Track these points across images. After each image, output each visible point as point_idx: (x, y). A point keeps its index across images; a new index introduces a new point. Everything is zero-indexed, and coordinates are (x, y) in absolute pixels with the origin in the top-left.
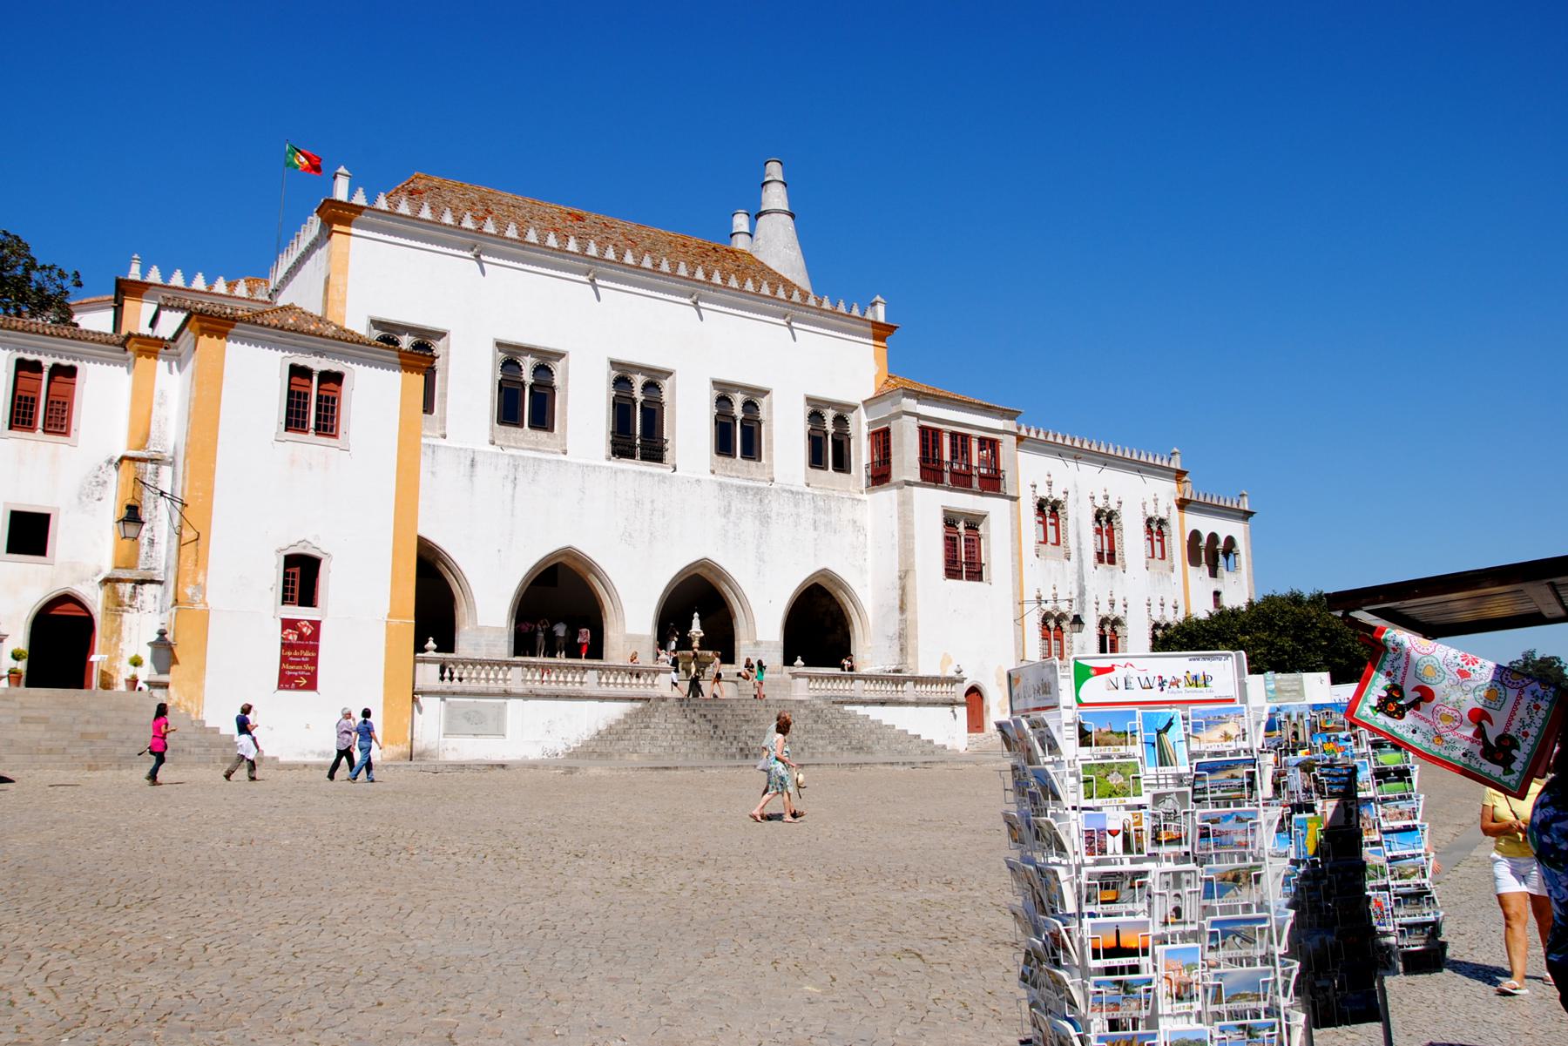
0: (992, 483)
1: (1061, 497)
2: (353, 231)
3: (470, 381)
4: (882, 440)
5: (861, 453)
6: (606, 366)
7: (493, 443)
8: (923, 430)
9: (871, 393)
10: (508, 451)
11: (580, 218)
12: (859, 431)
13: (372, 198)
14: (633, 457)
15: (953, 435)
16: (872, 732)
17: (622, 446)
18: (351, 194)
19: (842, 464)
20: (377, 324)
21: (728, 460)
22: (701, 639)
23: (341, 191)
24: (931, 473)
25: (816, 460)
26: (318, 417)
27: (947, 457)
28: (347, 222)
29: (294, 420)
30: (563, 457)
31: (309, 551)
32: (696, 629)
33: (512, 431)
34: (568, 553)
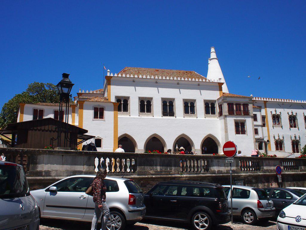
0: (246, 113)
1: (279, 114)
3: (134, 105)
4: (221, 107)
9: (219, 97)
10: (142, 117)
11: (158, 71)
12: (217, 106)
15: (236, 104)
17: (165, 114)
18: (110, 75)
19: (213, 113)
20: (116, 97)
21: (187, 114)
23: (108, 75)
24: (231, 112)
25: (207, 112)
29: (96, 116)
31: (99, 138)
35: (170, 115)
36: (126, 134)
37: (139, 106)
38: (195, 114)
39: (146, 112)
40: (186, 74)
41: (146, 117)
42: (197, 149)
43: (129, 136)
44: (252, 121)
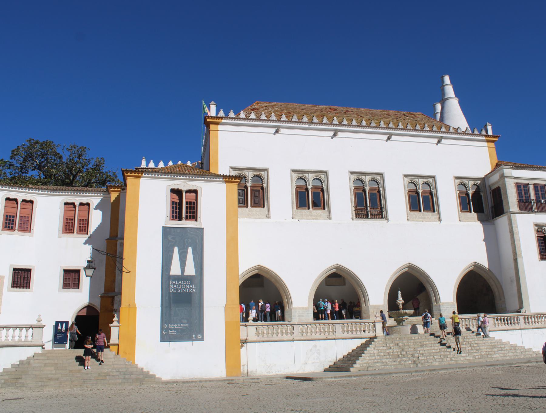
2: (220, 127)
5: (488, 202)
6: (347, 175)
8: (518, 186)
9: (490, 170)
11: (335, 110)
13: (227, 113)
14: (367, 217)
15: (536, 186)
16: (494, 347)
20: (235, 169)
22: (403, 304)
24: (525, 206)
26: (187, 212)
27: (533, 196)
28: (217, 124)
32: (400, 300)
33: (305, 212)
34: (338, 268)
35: (374, 216)
36: (260, 268)
37: (292, 194)
39: (313, 208)
40: (403, 116)
41: (312, 219)
42: (447, 303)
43: (268, 271)
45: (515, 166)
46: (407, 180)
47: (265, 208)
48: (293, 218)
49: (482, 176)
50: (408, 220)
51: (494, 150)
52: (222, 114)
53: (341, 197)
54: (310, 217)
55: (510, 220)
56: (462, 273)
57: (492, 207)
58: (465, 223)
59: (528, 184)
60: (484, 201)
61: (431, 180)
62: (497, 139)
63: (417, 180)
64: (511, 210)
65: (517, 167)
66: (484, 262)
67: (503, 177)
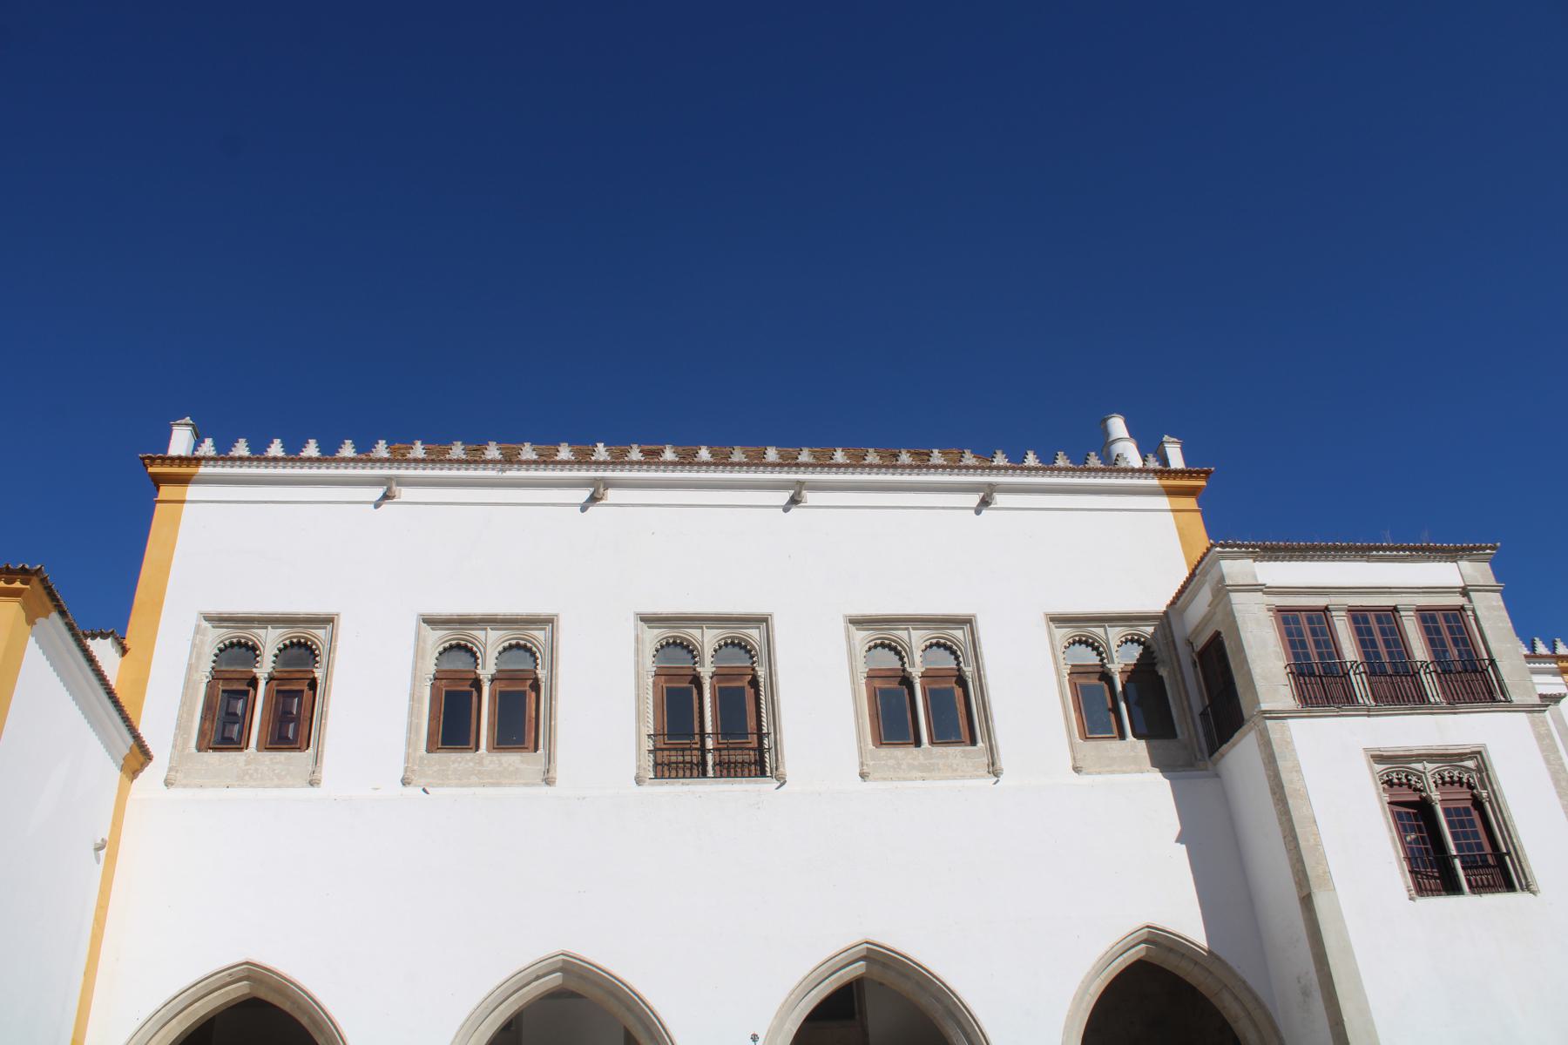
2: (192, 492)
5: (1187, 694)
7: (405, 782)
8: (1287, 618)
14: (704, 774)
15: (1358, 617)
28: (184, 480)
30: (547, 789)
35: (727, 769)
38: (980, 744)
43: (282, 985)
44: (1547, 761)
45: (1265, 549)
46: (862, 637)
47: (311, 750)
48: (405, 782)
49: (1158, 604)
50: (863, 776)
51: (1196, 520)
52: (208, 448)
53: (600, 701)
54: (474, 779)
55: (1266, 744)
56: (1098, 972)
57: (1203, 714)
58: (1099, 778)
59: (1326, 609)
60: (1170, 697)
61: (958, 634)
62: (1202, 483)
63: (903, 634)
64: (1264, 707)
65: (1272, 549)
66: (1190, 926)
67: (1222, 591)
